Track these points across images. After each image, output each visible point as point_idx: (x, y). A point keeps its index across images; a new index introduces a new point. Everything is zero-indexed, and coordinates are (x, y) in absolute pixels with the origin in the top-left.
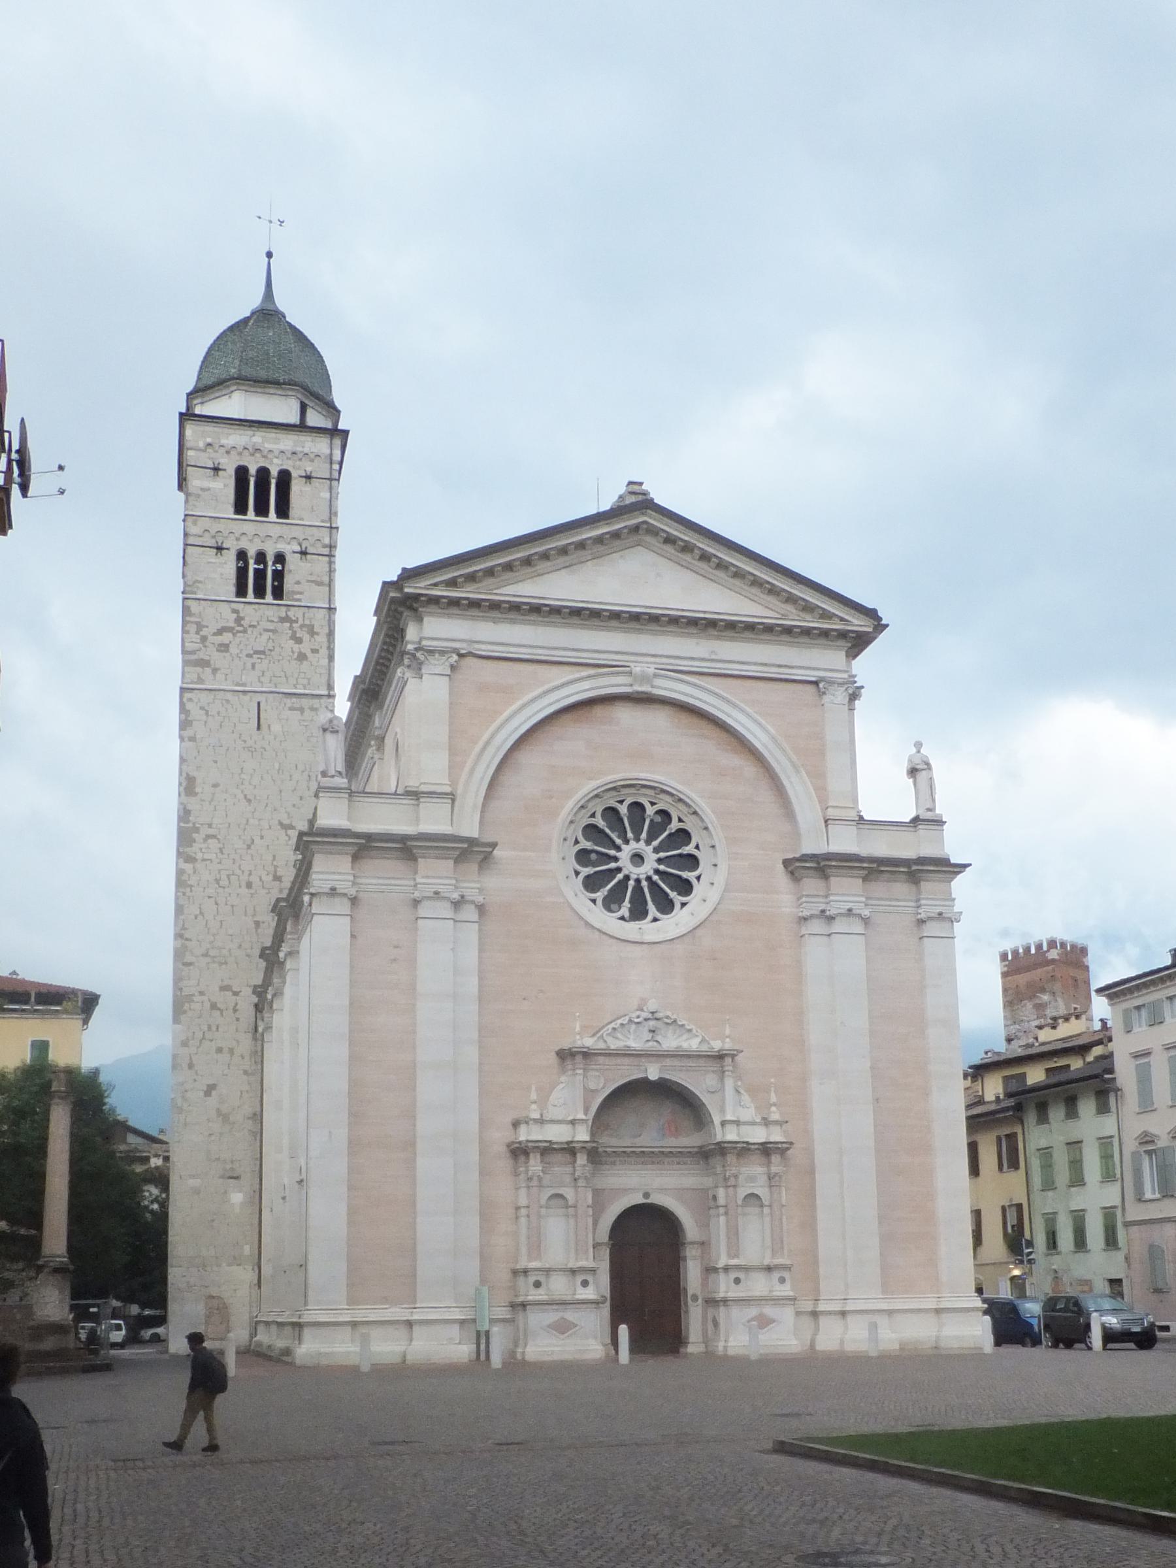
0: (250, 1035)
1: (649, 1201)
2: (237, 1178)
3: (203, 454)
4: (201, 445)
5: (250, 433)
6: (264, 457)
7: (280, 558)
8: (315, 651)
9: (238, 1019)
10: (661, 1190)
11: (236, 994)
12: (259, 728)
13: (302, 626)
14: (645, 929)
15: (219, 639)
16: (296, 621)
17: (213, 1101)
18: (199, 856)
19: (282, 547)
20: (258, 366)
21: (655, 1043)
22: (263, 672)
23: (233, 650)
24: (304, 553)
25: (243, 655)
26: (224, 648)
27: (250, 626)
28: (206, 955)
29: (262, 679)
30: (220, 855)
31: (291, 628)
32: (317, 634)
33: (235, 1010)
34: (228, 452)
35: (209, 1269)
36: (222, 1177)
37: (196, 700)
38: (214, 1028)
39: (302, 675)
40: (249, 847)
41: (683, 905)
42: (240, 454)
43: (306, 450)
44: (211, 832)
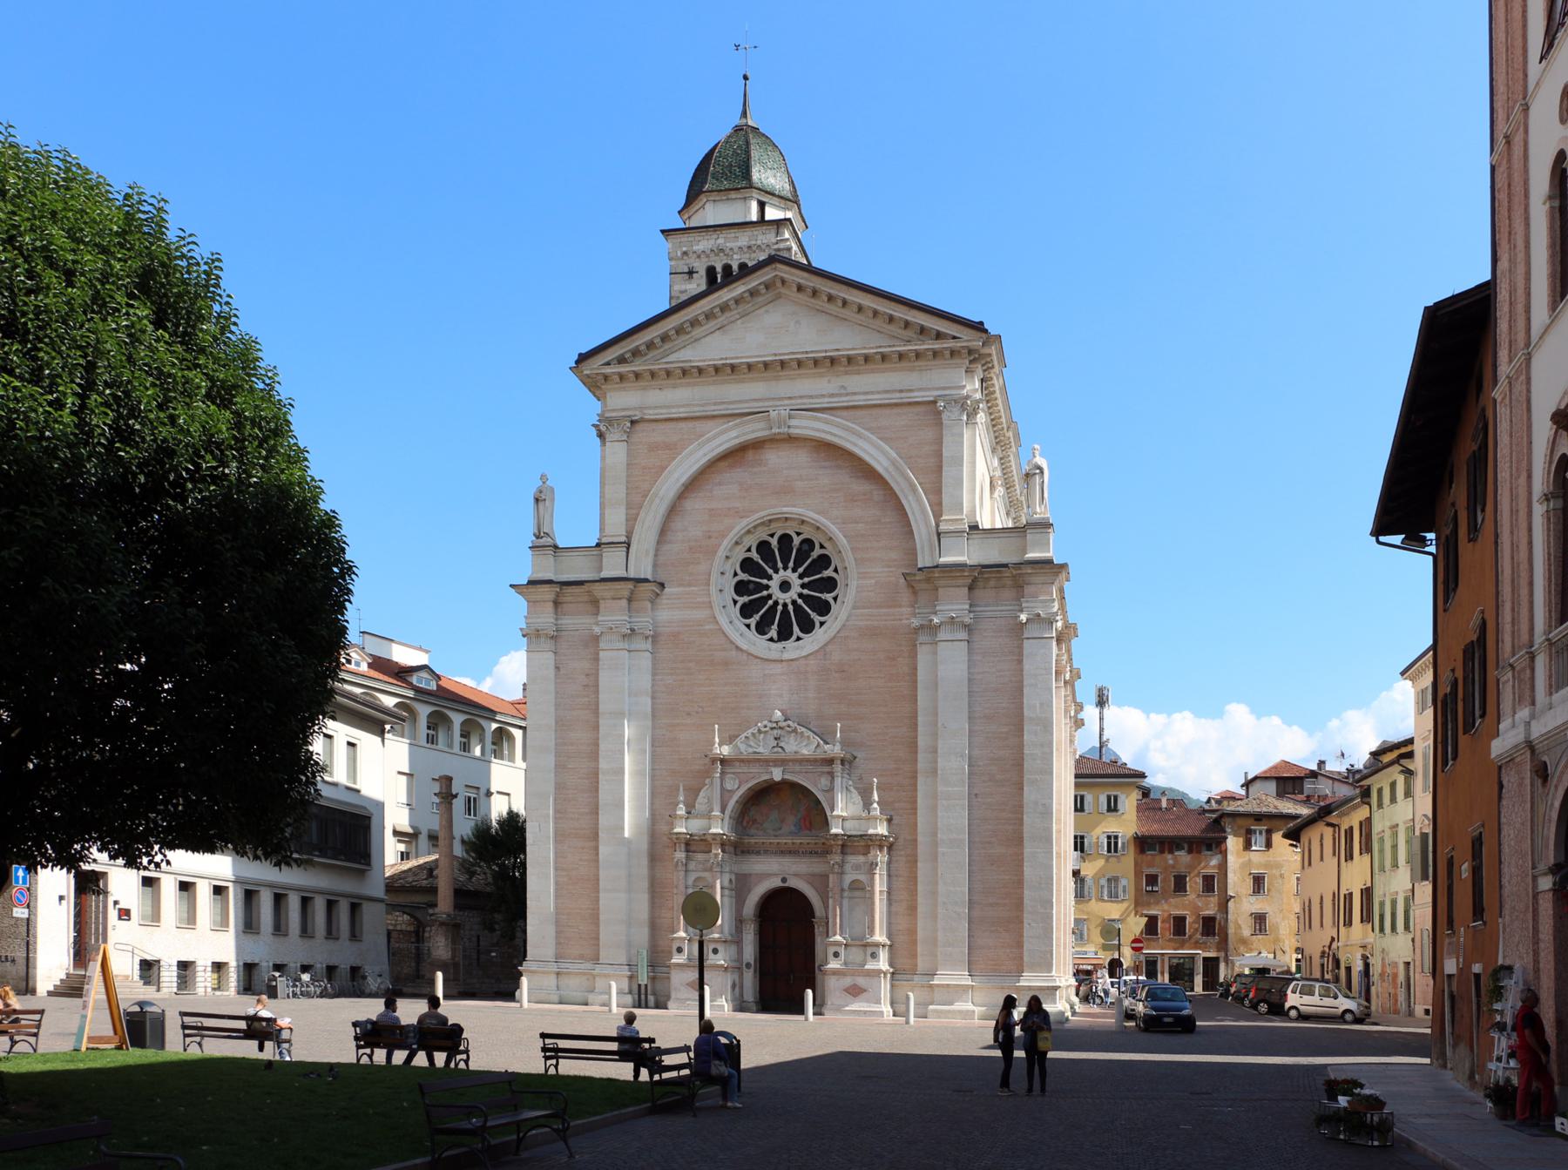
3: (683, 262)
5: (715, 236)
6: (727, 255)
14: (791, 649)
34: (699, 257)
42: (708, 256)
43: (759, 242)
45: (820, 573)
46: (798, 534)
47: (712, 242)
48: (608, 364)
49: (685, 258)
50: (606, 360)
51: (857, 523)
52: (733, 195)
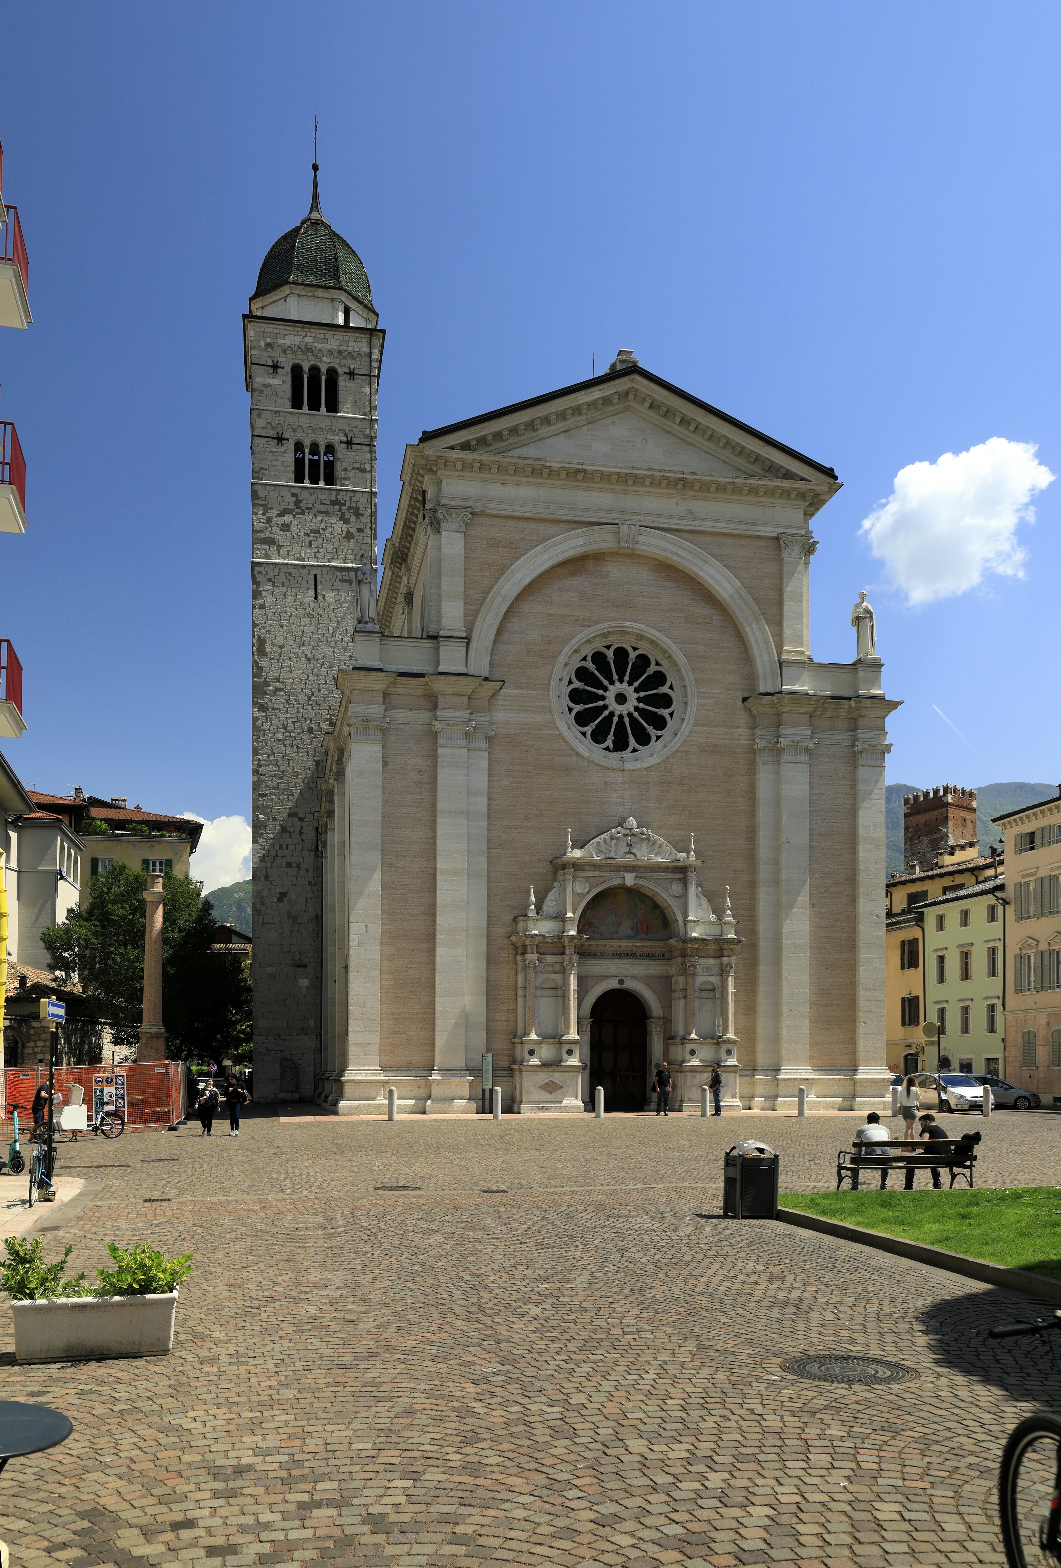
0: (312, 853)
1: (624, 986)
2: (305, 966)
3: (264, 354)
4: (262, 344)
6: (316, 356)
7: (330, 449)
8: (360, 530)
9: (303, 840)
10: (633, 977)
11: (301, 819)
12: (316, 598)
13: (349, 508)
15: (281, 520)
16: (345, 504)
17: (284, 906)
18: (270, 705)
19: (331, 438)
20: (307, 271)
21: (632, 856)
22: (318, 549)
23: (294, 529)
24: (349, 443)
25: (302, 534)
26: (286, 527)
27: (307, 508)
28: (277, 788)
29: (317, 554)
30: (286, 706)
31: (340, 510)
32: (362, 515)
33: (301, 833)
34: (284, 351)
35: (283, 1037)
36: (292, 966)
37: (264, 573)
38: (284, 847)
39: (350, 552)
40: (310, 699)
41: (658, 738)
42: (294, 353)
43: (350, 349)
44: (279, 685)
45: (656, 689)
46: (635, 649)
47: (299, 339)
48: (452, 448)
49: (269, 350)
50: (452, 444)
51: (697, 644)
52: (320, 293)
